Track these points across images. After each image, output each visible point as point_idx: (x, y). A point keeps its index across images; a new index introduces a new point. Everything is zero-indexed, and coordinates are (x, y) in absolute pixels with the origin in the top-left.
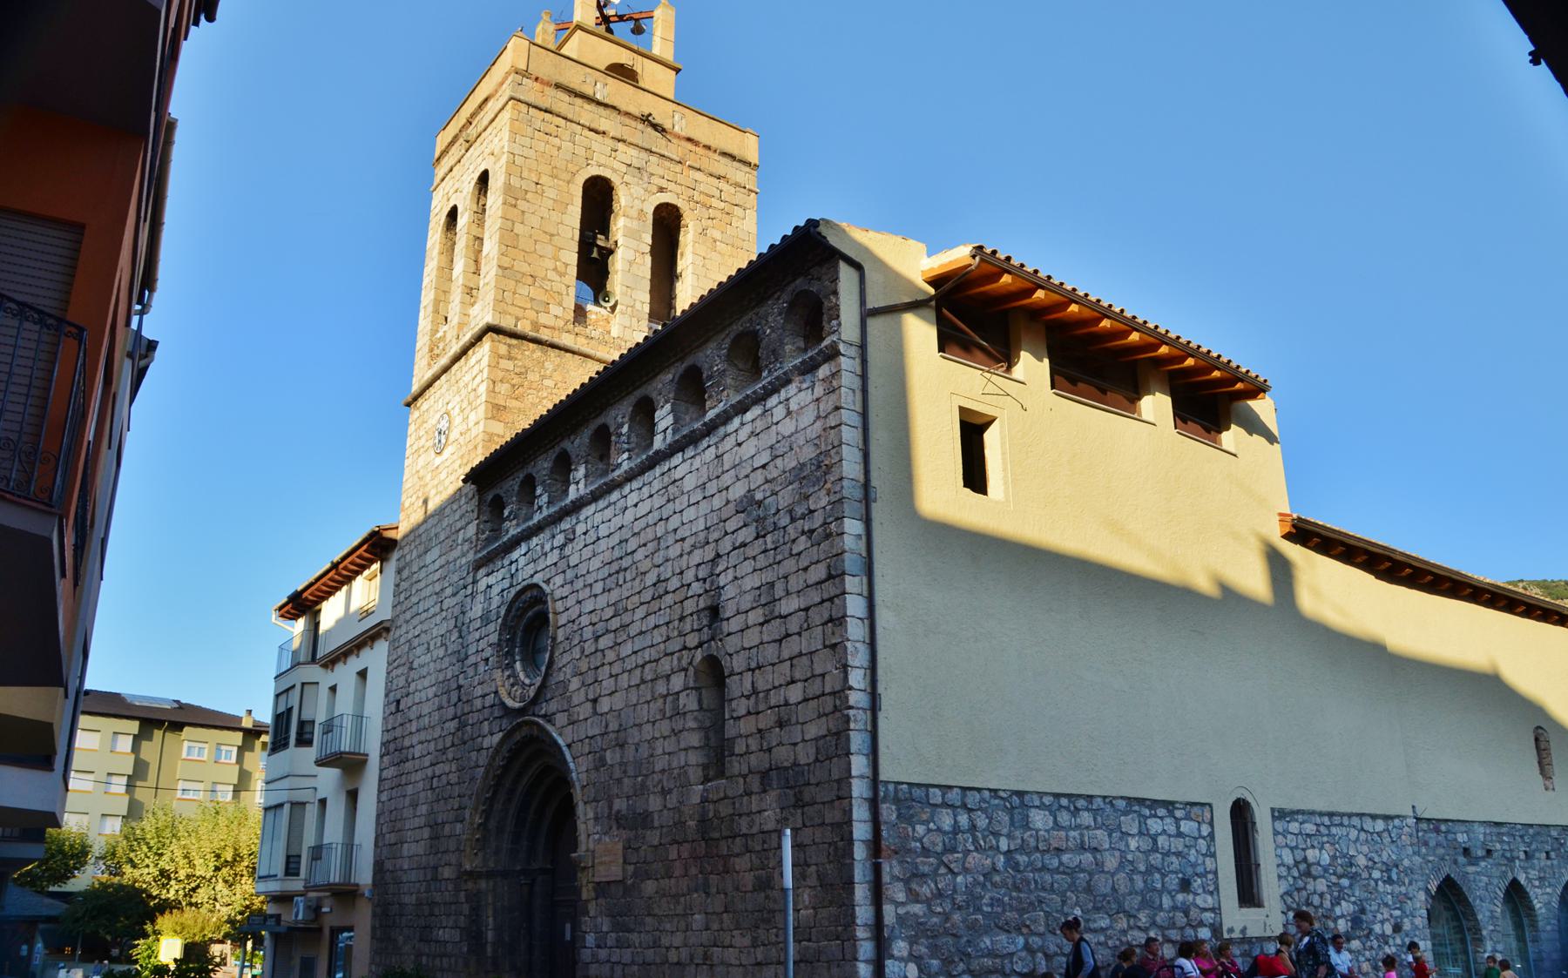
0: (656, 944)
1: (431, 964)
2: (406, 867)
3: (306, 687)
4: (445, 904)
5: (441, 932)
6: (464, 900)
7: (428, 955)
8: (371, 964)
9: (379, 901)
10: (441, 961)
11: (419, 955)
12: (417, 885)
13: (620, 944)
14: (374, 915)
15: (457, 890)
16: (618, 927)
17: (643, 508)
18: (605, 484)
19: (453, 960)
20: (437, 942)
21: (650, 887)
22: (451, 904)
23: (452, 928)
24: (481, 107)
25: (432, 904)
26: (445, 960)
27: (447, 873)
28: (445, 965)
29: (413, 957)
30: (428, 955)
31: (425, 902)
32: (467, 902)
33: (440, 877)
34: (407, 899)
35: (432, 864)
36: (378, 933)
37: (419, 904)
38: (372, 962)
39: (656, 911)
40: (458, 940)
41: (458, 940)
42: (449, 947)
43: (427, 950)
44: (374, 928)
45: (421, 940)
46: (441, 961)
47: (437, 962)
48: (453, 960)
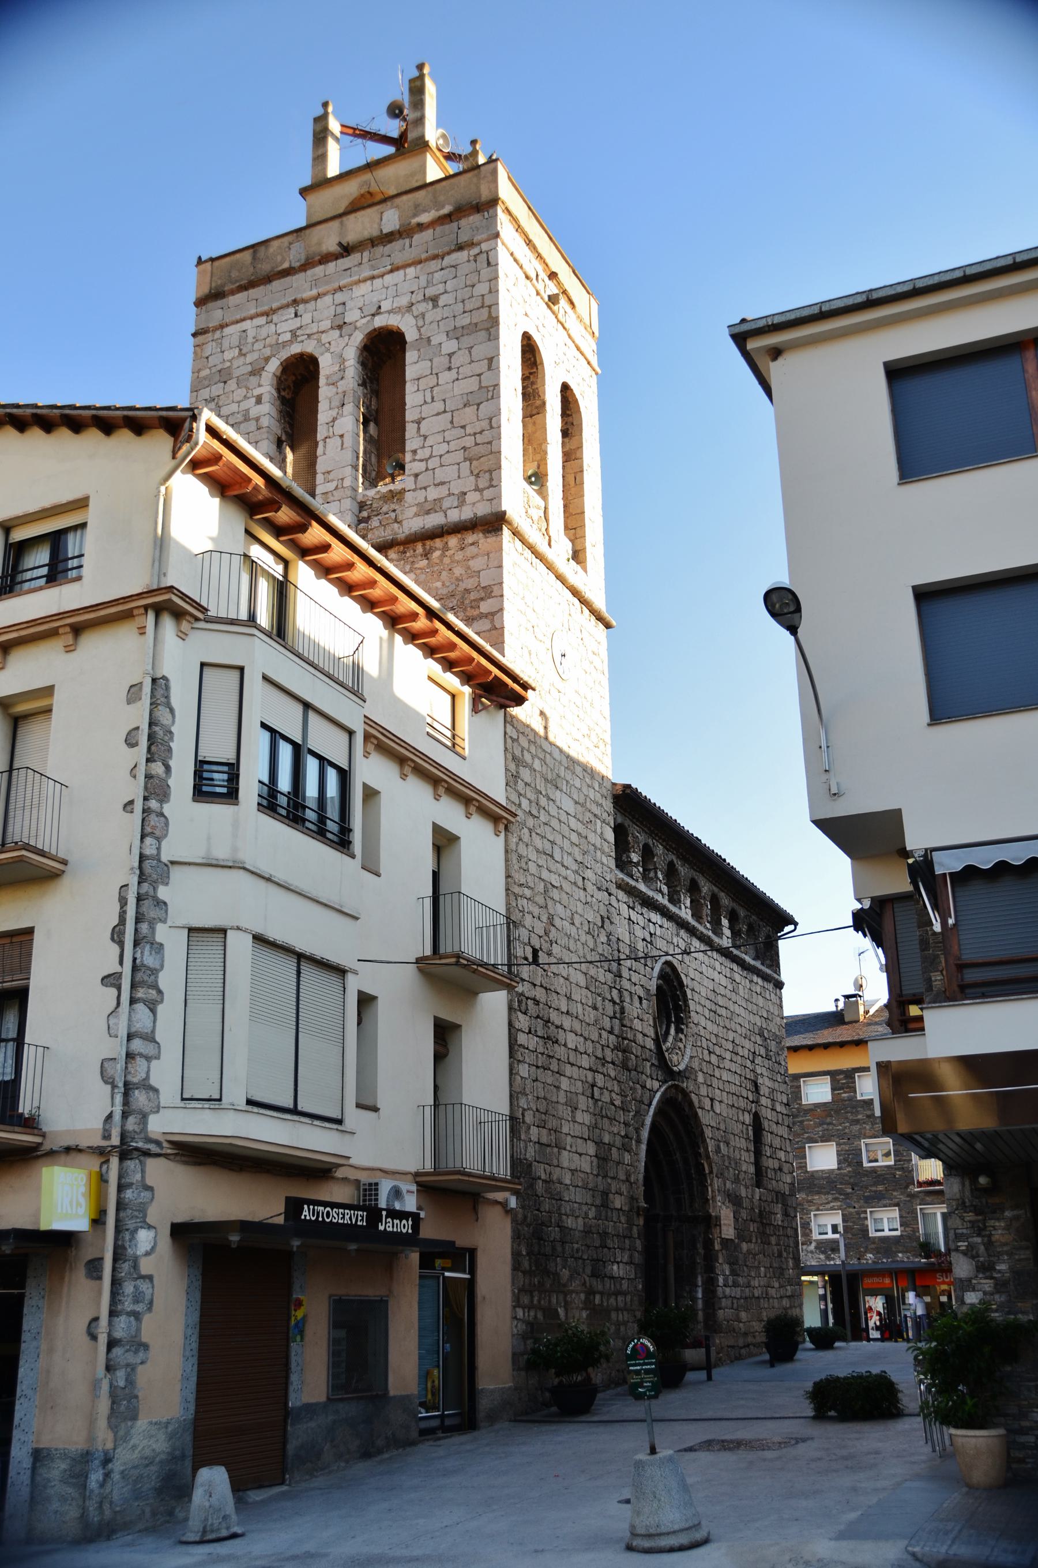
0: (749, 1286)
1: (605, 1304)
2: (568, 1182)
3: (206, 670)
4: (618, 1236)
5: (615, 1267)
6: (636, 1236)
7: (602, 1293)
8: (514, 1307)
9: (525, 1217)
10: (616, 1299)
11: (590, 1292)
12: (585, 1208)
13: (735, 1285)
14: (517, 1236)
15: (630, 1223)
16: (733, 1273)
17: (709, 972)
18: (709, 937)
19: (629, 1298)
20: (612, 1278)
21: (744, 1246)
22: (625, 1237)
23: (626, 1263)
24: (529, 242)
25: (603, 1236)
26: (620, 1298)
27: (618, 1202)
28: (621, 1305)
29: (582, 1296)
30: (602, 1293)
31: (594, 1230)
32: (639, 1238)
33: (611, 1205)
34: (570, 1222)
35: (601, 1188)
36: (526, 1264)
37: (587, 1232)
38: (517, 1303)
39: (748, 1263)
40: (633, 1276)
41: (633, 1276)
42: (625, 1285)
43: (600, 1288)
44: (516, 1255)
45: (594, 1275)
46: (616, 1300)
47: (612, 1300)
48: (629, 1298)
